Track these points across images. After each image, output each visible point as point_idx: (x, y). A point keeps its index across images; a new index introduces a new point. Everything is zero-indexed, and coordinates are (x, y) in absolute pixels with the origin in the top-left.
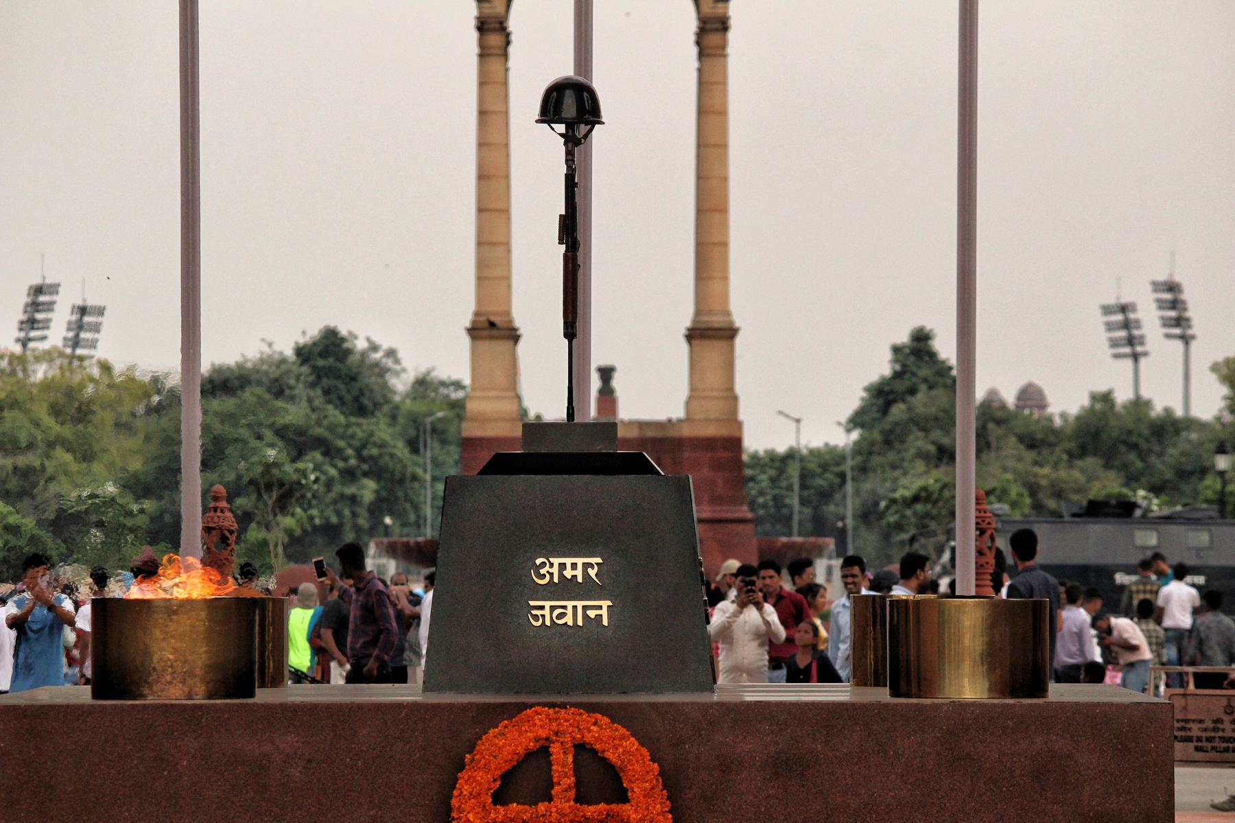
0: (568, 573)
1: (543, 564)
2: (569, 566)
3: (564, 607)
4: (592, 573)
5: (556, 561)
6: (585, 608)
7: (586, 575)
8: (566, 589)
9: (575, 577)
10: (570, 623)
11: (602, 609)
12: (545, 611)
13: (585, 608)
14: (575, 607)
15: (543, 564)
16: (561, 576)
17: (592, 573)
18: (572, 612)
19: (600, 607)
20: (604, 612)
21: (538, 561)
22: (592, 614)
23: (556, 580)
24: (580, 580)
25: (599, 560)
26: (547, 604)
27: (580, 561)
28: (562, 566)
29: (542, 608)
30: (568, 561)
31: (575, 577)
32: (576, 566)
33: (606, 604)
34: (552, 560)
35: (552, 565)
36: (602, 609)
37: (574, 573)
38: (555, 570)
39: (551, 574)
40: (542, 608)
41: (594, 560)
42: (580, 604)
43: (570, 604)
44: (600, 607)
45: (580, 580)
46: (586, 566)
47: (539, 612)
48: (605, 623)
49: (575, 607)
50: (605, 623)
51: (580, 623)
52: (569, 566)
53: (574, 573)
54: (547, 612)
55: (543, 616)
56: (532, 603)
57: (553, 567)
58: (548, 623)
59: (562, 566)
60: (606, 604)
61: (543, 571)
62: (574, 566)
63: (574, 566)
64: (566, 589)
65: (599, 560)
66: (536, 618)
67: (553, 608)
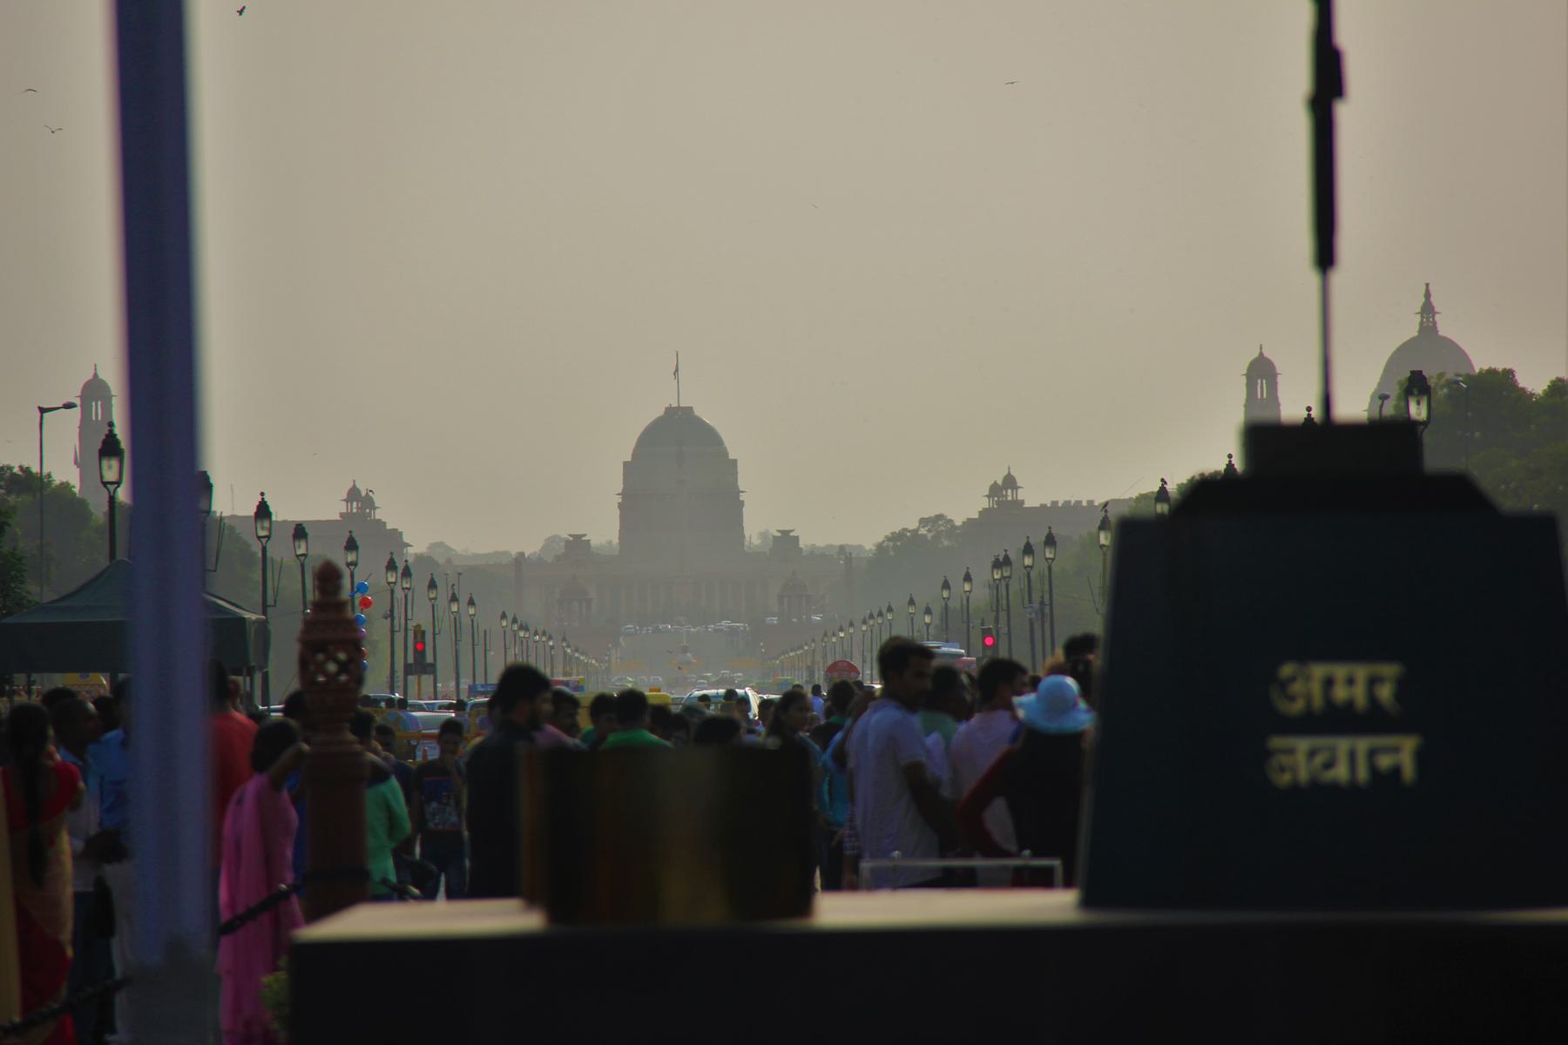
0: (1340, 693)
1: (1293, 679)
4: (1385, 693)
5: (1319, 671)
7: (1373, 699)
8: (1335, 719)
11: (1403, 754)
12: (1300, 759)
13: (1372, 753)
18: (1345, 760)
19: (1396, 750)
21: (1287, 670)
22: (1385, 762)
23: (1318, 702)
26: (1303, 744)
27: (1361, 672)
28: (1329, 683)
30: (1340, 671)
36: (1403, 754)
38: (1316, 689)
41: (1390, 670)
42: (1363, 744)
43: (1343, 745)
46: (1373, 682)
54: (1301, 758)
56: (1277, 742)
59: (1329, 683)
62: (1351, 681)
63: (1351, 681)
64: (1335, 719)
67: (1312, 754)
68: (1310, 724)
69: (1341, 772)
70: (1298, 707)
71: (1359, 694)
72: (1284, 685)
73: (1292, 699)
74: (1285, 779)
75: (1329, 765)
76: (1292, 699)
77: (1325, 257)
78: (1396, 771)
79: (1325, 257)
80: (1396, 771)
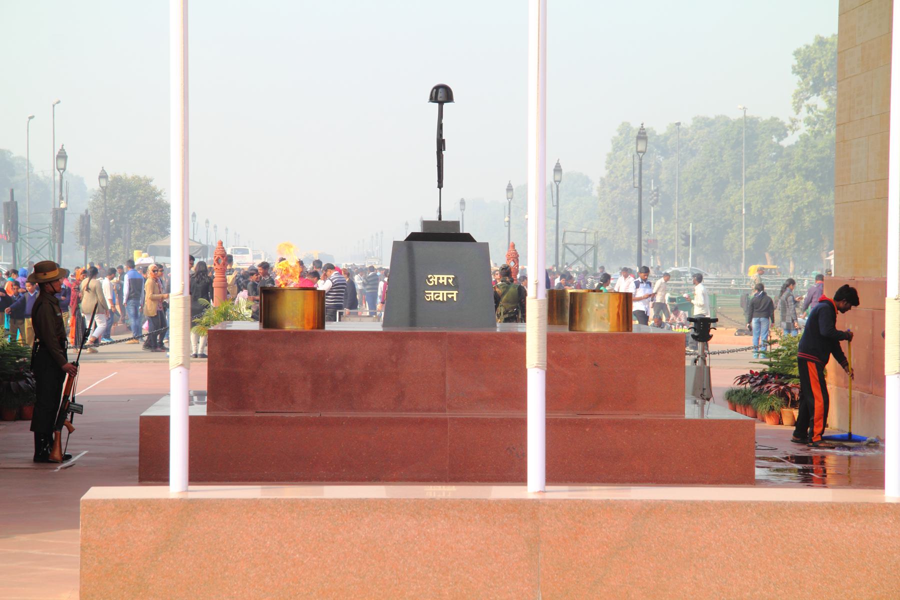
0: (441, 281)
4: (450, 281)
5: (436, 276)
8: (440, 287)
11: (454, 294)
12: (431, 295)
17: (450, 281)
18: (442, 295)
20: (455, 296)
22: (450, 296)
26: (432, 292)
27: (446, 277)
28: (439, 278)
30: (441, 276)
32: (444, 279)
33: (455, 292)
36: (454, 294)
38: (436, 280)
42: (445, 292)
43: (441, 292)
46: (448, 278)
57: (434, 279)
59: (439, 278)
64: (440, 287)
68: (434, 288)
69: (441, 298)
72: (429, 279)
77: (440, 186)
79: (440, 186)
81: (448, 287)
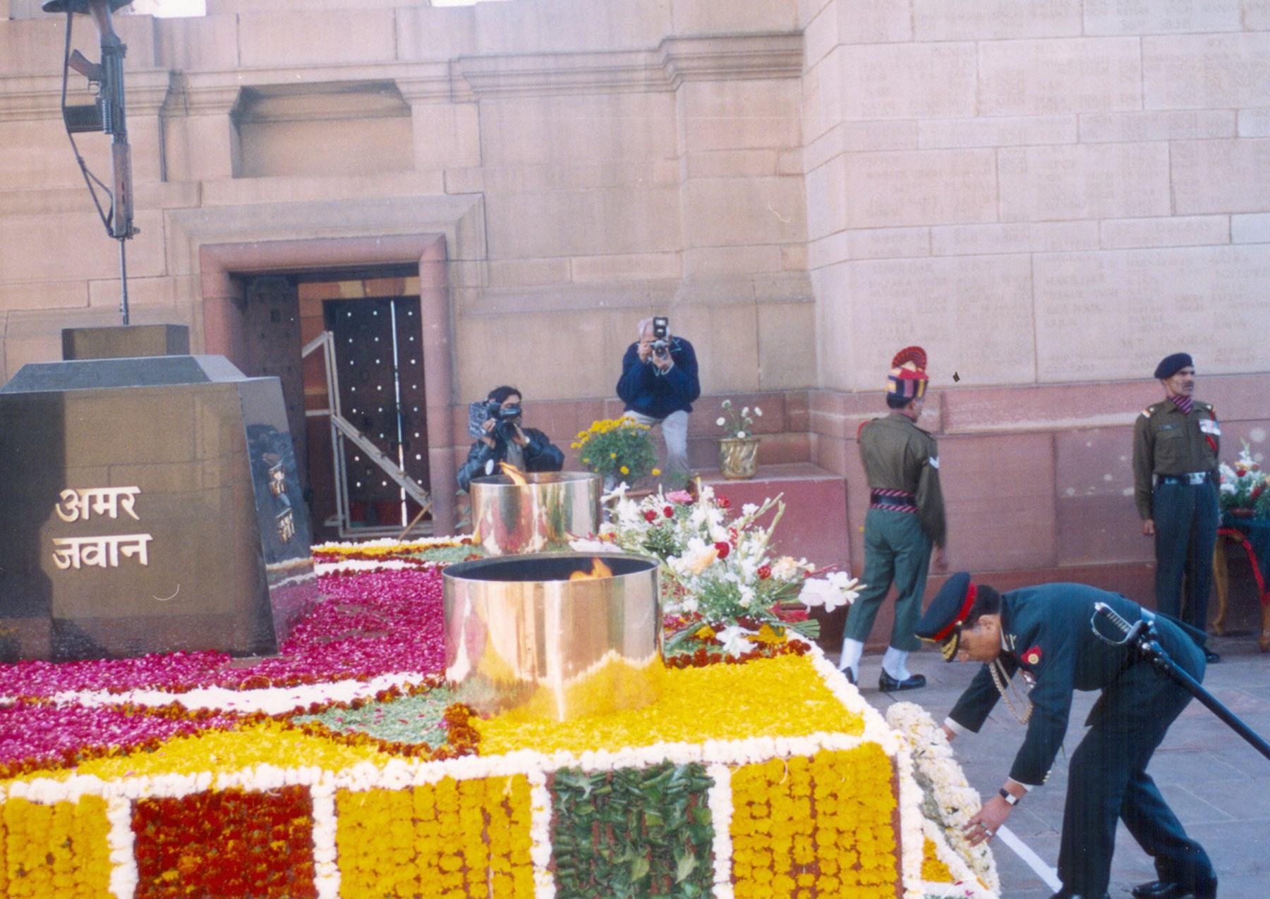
0: (100, 507)
1: (70, 498)
2: (100, 499)
3: (95, 545)
4: (128, 505)
5: (87, 493)
6: (120, 545)
7: (120, 509)
8: (98, 525)
9: (106, 512)
10: (103, 564)
13: (120, 545)
14: (108, 545)
15: (70, 498)
16: (91, 511)
18: (104, 550)
19: (136, 543)
20: (142, 549)
21: (65, 494)
22: (128, 551)
23: (86, 516)
24: (113, 514)
25: (136, 490)
26: (75, 542)
27: (113, 492)
28: (92, 500)
29: (69, 547)
30: (99, 492)
31: (106, 512)
32: (109, 499)
33: (143, 538)
34: (81, 492)
35: (80, 498)
37: (107, 506)
38: (85, 504)
39: (80, 510)
40: (69, 547)
41: (132, 490)
42: (114, 540)
43: (101, 541)
44: (136, 543)
45: (113, 514)
46: (121, 497)
47: (65, 553)
48: (144, 560)
49: (108, 545)
50: (144, 560)
51: (114, 562)
52: (100, 499)
53: (107, 506)
54: (75, 551)
55: (70, 557)
58: (77, 564)
59: (92, 500)
60: (143, 538)
61: (71, 505)
62: (106, 499)
63: (106, 499)
64: (98, 525)
65: (136, 490)
66: (62, 559)
67: (82, 547)
69: (100, 560)
70: (74, 517)
71: (112, 507)
73: (70, 512)
74: (66, 565)
75: (91, 555)
76: (70, 512)
78: (136, 555)
80: (136, 555)
81: (121, 525)
